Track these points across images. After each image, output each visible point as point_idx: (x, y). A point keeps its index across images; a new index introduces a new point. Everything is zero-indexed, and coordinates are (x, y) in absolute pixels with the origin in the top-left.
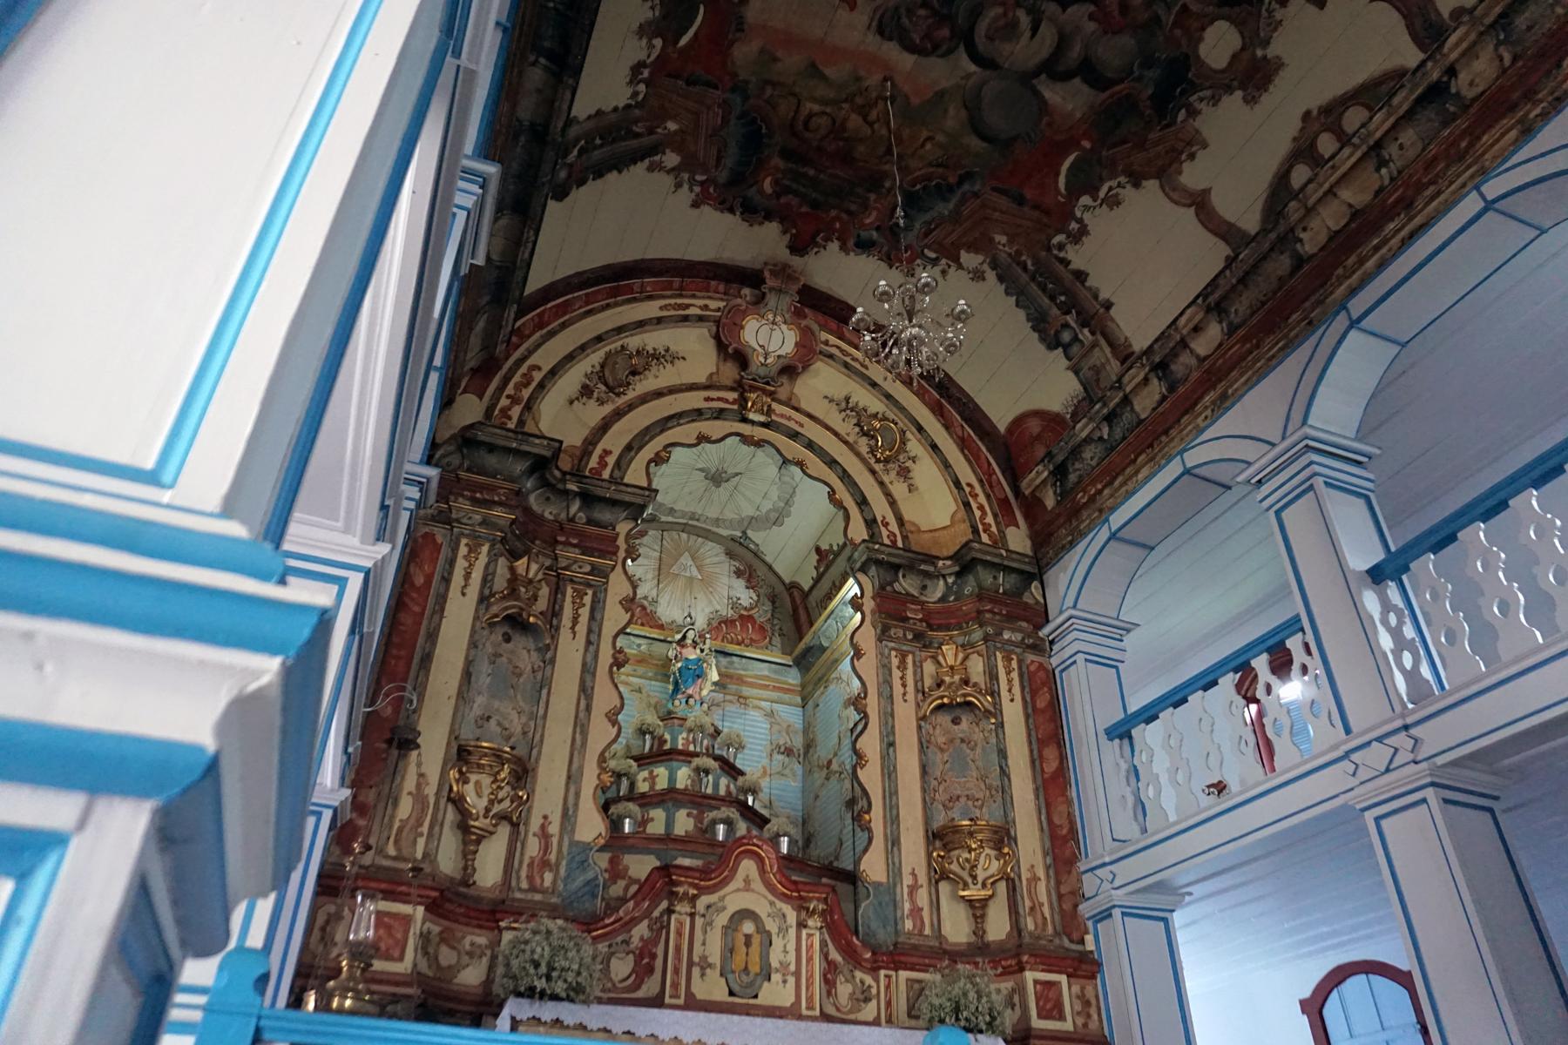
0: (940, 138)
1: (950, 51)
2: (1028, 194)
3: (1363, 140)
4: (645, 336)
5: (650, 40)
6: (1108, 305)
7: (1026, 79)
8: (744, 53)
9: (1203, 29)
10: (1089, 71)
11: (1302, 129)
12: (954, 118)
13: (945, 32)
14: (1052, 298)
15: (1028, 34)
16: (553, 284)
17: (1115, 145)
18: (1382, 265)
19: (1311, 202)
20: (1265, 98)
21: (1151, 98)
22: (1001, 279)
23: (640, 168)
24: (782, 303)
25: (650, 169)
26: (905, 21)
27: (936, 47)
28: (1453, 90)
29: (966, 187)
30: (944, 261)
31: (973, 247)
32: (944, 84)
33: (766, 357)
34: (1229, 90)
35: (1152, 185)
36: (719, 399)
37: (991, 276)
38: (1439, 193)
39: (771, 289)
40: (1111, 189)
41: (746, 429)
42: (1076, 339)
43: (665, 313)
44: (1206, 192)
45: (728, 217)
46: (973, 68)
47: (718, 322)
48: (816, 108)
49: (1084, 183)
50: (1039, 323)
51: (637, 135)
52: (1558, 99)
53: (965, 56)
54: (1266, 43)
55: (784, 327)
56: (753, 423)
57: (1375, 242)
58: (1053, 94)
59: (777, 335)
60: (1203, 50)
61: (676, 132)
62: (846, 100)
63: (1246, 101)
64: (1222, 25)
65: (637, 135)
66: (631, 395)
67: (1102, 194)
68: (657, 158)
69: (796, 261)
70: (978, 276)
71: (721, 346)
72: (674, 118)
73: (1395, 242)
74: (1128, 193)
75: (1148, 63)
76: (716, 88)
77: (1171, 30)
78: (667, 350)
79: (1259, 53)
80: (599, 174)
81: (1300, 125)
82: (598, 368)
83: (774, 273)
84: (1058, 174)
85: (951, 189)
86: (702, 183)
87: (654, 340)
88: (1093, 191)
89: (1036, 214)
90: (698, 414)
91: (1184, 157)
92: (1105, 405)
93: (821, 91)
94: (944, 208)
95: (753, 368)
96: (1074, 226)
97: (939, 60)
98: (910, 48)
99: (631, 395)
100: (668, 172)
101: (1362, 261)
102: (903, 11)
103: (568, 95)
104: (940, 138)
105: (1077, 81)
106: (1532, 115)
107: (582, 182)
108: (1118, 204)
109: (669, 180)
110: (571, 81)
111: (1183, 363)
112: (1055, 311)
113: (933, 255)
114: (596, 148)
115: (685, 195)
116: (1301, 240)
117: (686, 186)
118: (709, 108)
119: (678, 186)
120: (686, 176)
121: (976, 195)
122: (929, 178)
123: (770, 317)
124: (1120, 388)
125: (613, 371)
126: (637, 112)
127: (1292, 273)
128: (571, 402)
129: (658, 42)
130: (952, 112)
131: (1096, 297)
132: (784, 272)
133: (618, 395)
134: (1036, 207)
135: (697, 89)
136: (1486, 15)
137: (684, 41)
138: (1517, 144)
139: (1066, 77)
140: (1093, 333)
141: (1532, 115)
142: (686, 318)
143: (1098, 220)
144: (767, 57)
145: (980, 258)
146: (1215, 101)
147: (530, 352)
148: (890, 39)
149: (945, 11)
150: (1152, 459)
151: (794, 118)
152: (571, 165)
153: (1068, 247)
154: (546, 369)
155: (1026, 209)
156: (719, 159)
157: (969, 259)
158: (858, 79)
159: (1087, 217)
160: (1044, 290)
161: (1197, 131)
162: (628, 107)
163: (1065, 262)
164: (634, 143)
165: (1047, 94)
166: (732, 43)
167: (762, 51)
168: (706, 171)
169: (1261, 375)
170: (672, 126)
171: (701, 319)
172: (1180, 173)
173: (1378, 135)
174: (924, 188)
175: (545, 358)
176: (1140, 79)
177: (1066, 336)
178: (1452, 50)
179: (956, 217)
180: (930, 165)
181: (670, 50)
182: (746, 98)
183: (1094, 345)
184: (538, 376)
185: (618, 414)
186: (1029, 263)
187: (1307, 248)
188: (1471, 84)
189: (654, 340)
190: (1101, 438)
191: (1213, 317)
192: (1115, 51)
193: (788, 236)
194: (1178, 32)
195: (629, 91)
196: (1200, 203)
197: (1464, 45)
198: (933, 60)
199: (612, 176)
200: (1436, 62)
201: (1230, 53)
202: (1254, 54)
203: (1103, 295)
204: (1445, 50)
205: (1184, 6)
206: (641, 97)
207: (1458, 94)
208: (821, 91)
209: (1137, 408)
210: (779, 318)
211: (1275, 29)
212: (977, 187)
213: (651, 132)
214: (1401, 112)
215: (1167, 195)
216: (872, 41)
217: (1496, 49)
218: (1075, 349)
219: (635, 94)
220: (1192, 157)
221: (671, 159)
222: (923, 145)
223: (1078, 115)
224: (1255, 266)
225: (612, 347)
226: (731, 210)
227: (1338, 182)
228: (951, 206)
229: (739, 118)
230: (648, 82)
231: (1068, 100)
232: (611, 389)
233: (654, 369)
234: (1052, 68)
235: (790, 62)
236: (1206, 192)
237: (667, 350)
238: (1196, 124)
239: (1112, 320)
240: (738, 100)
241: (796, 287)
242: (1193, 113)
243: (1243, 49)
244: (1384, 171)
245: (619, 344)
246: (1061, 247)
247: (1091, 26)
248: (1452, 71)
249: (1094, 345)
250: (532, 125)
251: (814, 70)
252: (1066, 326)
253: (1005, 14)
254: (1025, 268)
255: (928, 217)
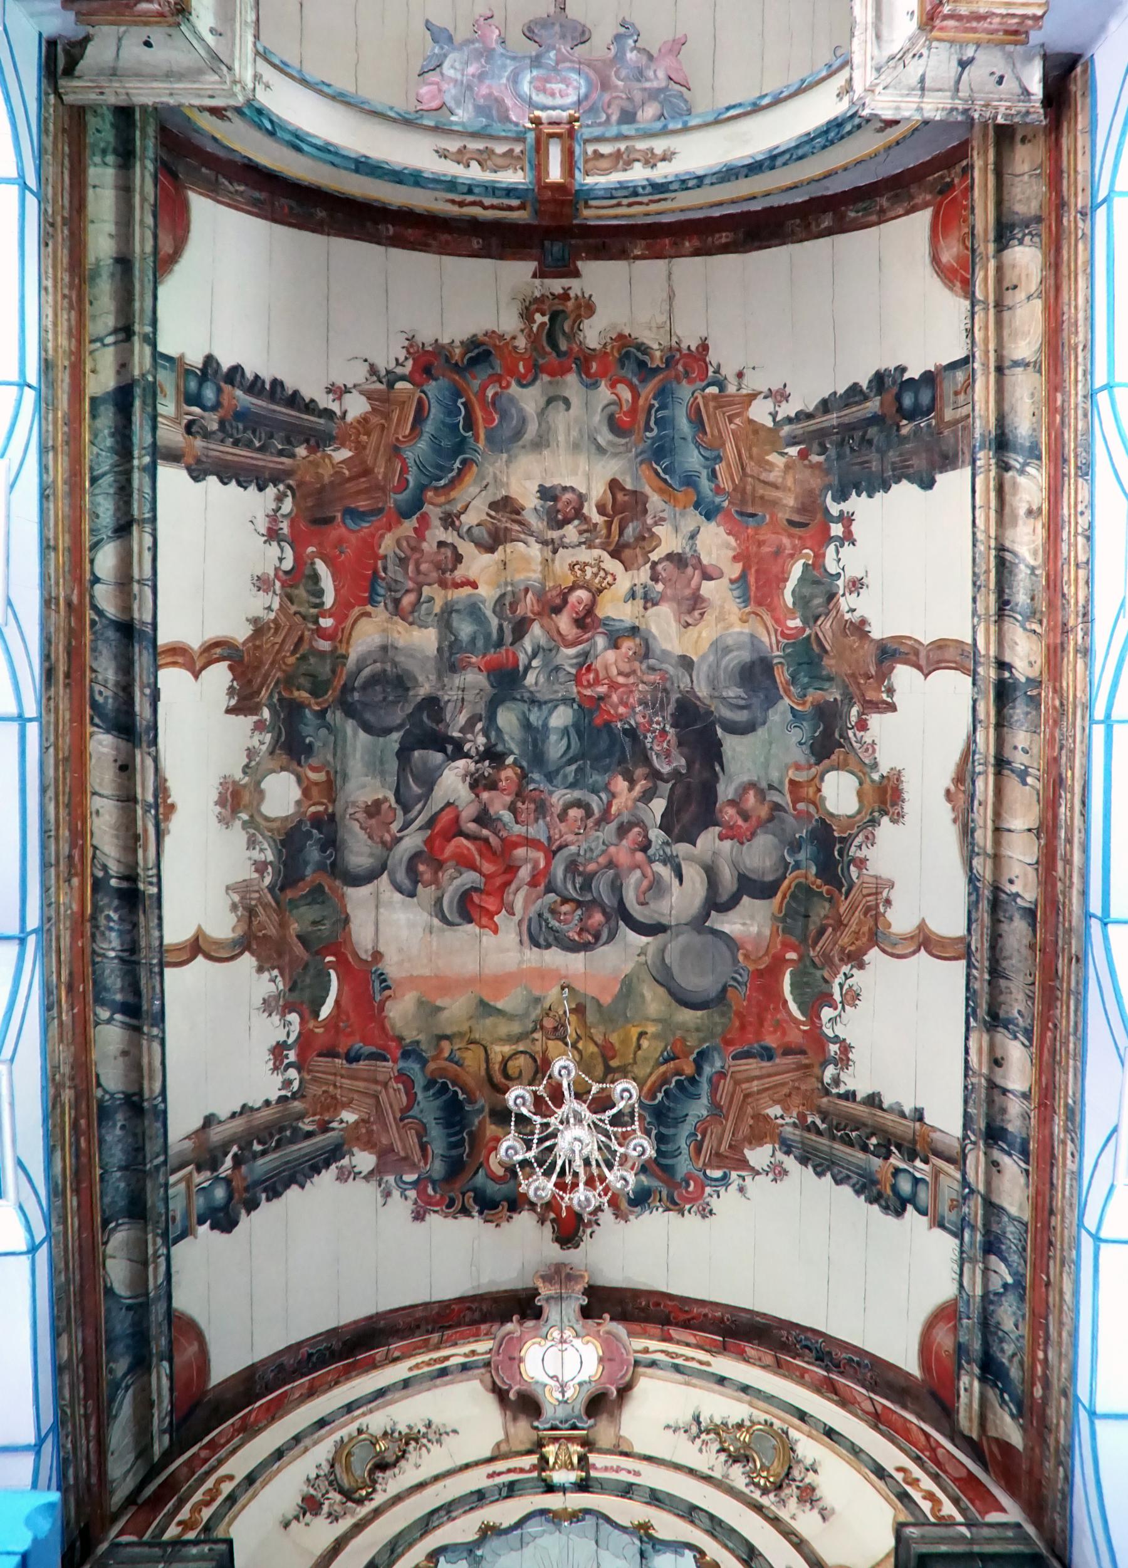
0: (651, 1029)
1: (612, 937)
2: (771, 1041)
3: (985, 764)
4: (390, 1410)
5: (283, 1015)
6: (919, 1115)
7: (699, 923)
8: (400, 1012)
9: (819, 790)
10: (754, 887)
11: (953, 809)
12: (653, 1000)
13: (598, 917)
14: (865, 1148)
15: (676, 882)
16: (252, 1369)
17: (815, 943)
18: (1085, 849)
19: (990, 850)
20: (907, 807)
21: (817, 875)
22: (803, 1161)
23: (328, 1176)
24: (563, 1313)
25: (342, 1177)
26: (554, 923)
27: (597, 937)
28: (1023, 680)
29: (708, 1070)
30: (734, 1175)
31: (756, 1139)
32: (628, 968)
33: (563, 1388)
34: (874, 822)
35: (874, 955)
36: (509, 1471)
37: (790, 1163)
38: (1072, 751)
39: (548, 1299)
40: (841, 985)
41: (553, 1501)
42: (916, 1181)
43: (416, 1372)
44: (922, 926)
45: (464, 1221)
46: (645, 939)
47: (487, 1364)
48: (507, 1049)
49: (815, 998)
50: (869, 1188)
51: (309, 1135)
52: (1085, 615)
53: (628, 930)
54: (875, 766)
55: (577, 1342)
56: (563, 1489)
57: (1063, 835)
58: (731, 924)
59: (571, 1356)
60: (831, 806)
61: (356, 1123)
62: (534, 1030)
63: (893, 821)
64: (831, 777)
65: (309, 1135)
66: (379, 1499)
67: (837, 997)
68: (345, 1162)
69: (572, 1256)
70: (778, 1173)
71: (501, 1395)
72: (346, 1106)
73: (1078, 821)
74: (859, 979)
75: (795, 846)
76: (385, 1060)
77: (795, 809)
78: (429, 1425)
79: (876, 777)
80: (274, 1193)
81: (949, 806)
82: (326, 1468)
83: (547, 1279)
84: (786, 1002)
85: (693, 1081)
86: (415, 1184)
87: (405, 1413)
88: (827, 999)
89: (790, 1060)
90: (480, 1497)
91: (882, 909)
92: (973, 1228)
93: (505, 1028)
94: (699, 1109)
95: (548, 1412)
96: (834, 1048)
97: (606, 948)
98: (574, 947)
99: (379, 1499)
100: (367, 1178)
101: (1068, 862)
102: (547, 915)
103: (156, 1046)
104: (651, 1029)
105: (746, 899)
106: (1080, 641)
107: (252, 1206)
108: (857, 996)
109: (368, 1191)
110: (155, 1031)
111: (1016, 1114)
112: (877, 1162)
113: (718, 1174)
114: (255, 1156)
115: (401, 1207)
116: (1017, 895)
117: (396, 1194)
118: (385, 1085)
119: (387, 1194)
120: (391, 1179)
121: (722, 1075)
122: (665, 1080)
123: (556, 1334)
124: (972, 1191)
125: (348, 1468)
126: (297, 1105)
127: (1033, 925)
128: (286, 1525)
129: (294, 1018)
130: (648, 995)
131: (902, 1115)
132: (560, 1274)
133: (360, 1502)
134: (788, 1051)
135: (362, 1065)
136: (987, 608)
137: (325, 1011)
138: (1088, 666)
139: (732, 903)
140: (926, 1161)
141: (1080, 641)
142: (443, 1372)
143: (845, 1025)
144: (429, 1010)
145: (768, 1148)
146: (871, 840)
147: (221, 1462)
148: (548, 946)
149: (589, 897)
150: (1063, 1264)
151: (488, 1069)
152: (228, 1181)
153: (843, 1077)
154: (240, 1476)
155: (777, 1061)
156: (423, 1148)
157: (759, 1156)
158: (538, 1000)
159: (840, 1031)
160: (850, 1143)
161: (876, 877)
162: (282, 1099)
163: (850, 1096)
164: (305, 1145)
165: (726, 928)
166: (382, 1008)
167: (421, 1003)
168: (414, 1167)
169: (1081, 1056)
170: (349, 1117)
171: (464, 1367)
172: (889, 926)
173: (992, 751)
174: (667, 1093)
175: (239, 1465)
176: (797, 866)
177: (905, 1186)
178: (987, 649)
179: (717, 1111)
180: (659, 1064)
181: (311, 1024)
182: (424, 1062)
183: (937, 1173)
184: (227, 1488)
185: (359, 1527)
186: (818, 1122)
187: (1027, 896)
188: (1031, 664)
189: (405, 1413)
190: (1005, 1286)
191: (1002, 1036)
192: (760, 855)
193: (548, 1224)
194: (801, 806)
195: (278, 1079)
196: (924, 941)
197: (993, 638)
198: (602, 950)
199: (294, 1191)
200: (982, 664)
201: (854, 794)
202: (873, 781)
203: (907, 1109)
204: (983, 652)
205: (792, 782)
206: (296, 1085)
207: (1028, 679)
208: (505, 1028)
209: (1013, 1210)
210: (568, 1333)
211: (874, 751)
212: (718, 1064)
213: (325, 1128)
214: (993, 720)
215: (892, 955)
216: (533, 957)
217: (1025, 629)
218: (923, 1195)
219: (287, 1083)
220: (888, 902)
221: (365, 1160)
222: (639, 1047)
223: (767, 932)
224: (993, 947)
225: (344, 1432)
226: (465, 1212)
227: (997, 815)
228: (704, 1100)
229: (426, 1088)
230: (299, 1066)
231: (749, 922)
232: (348, 1495)
233: (412, 1456)
234: (717, 902)
235: (456, 1010)
236: (922, 926)
237: (429, 1425)
238: (871, 872)
239: (934, 1129)
240: (416, 1067)
241: (580, 1287)
242: (861, 863)
243: (861, 784)
244: (1029, 780)
245: (352, 1428)
246: (837, 1081)
247: (727, 844)
248: (1002, 665)
249: (937, 1173)
250: (128, 1097)
251: (485, 1008)
252: (897, 1171)
253: (644, 875)
254: (819, 1133)
255: (686, 1129)
